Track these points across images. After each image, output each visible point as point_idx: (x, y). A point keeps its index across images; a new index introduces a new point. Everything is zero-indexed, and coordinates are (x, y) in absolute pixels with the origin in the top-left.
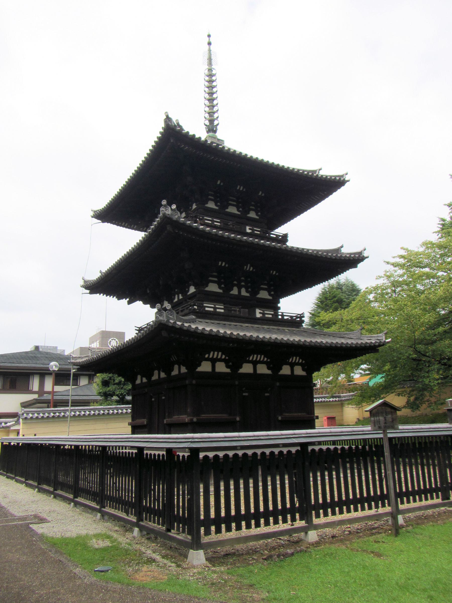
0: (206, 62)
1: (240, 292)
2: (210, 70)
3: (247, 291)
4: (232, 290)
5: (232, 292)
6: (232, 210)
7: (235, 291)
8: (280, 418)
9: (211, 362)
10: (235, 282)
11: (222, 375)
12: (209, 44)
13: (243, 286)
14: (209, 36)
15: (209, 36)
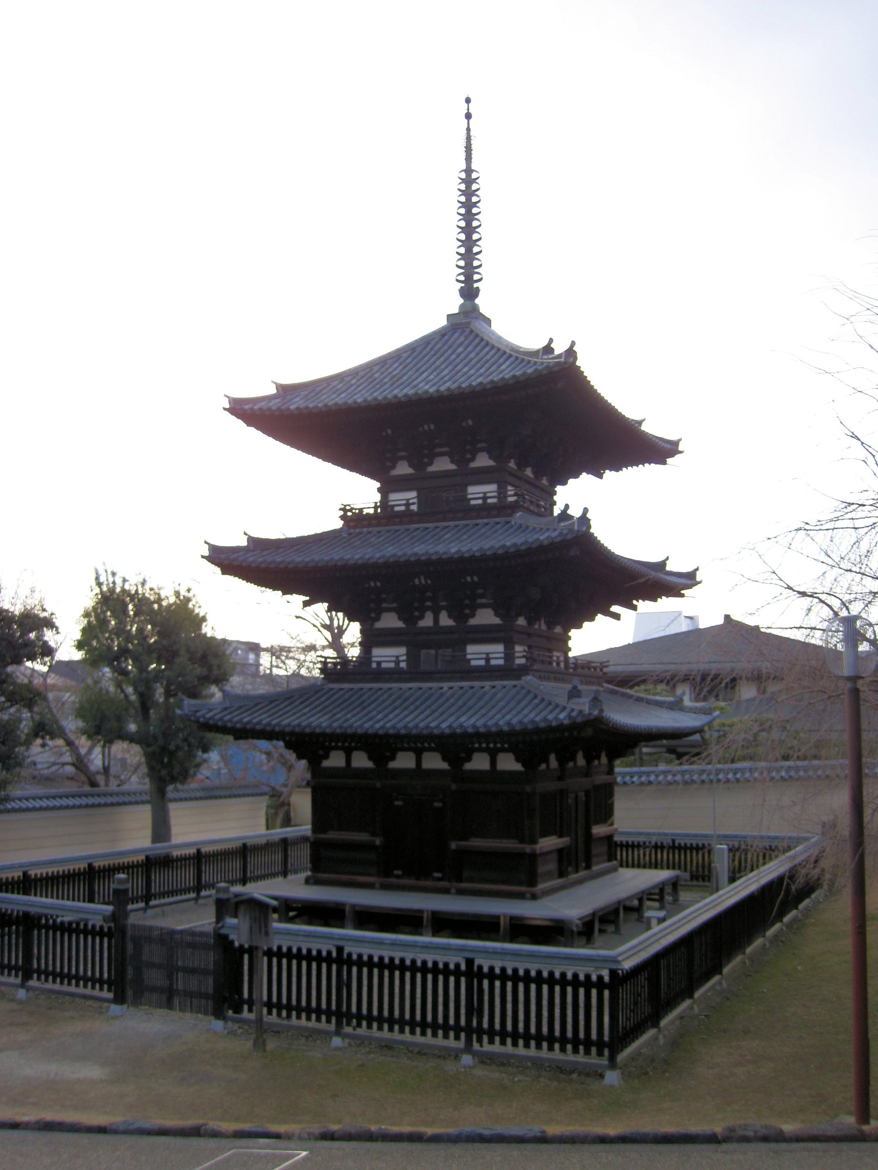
0: (463, 155)
1: (436, 620)
2: (469, 171)
3: (450, 616)
4: (422, 617)
5: (422, 624)
6: (443, 464)
7: (427, 621)
8: (453, 845)
9: (345, 752)
10: (429, 604)
11: (362, 773)
12: (468, 116)
13: (442, 608)
14: (468, 101)
15: (468, 101)
